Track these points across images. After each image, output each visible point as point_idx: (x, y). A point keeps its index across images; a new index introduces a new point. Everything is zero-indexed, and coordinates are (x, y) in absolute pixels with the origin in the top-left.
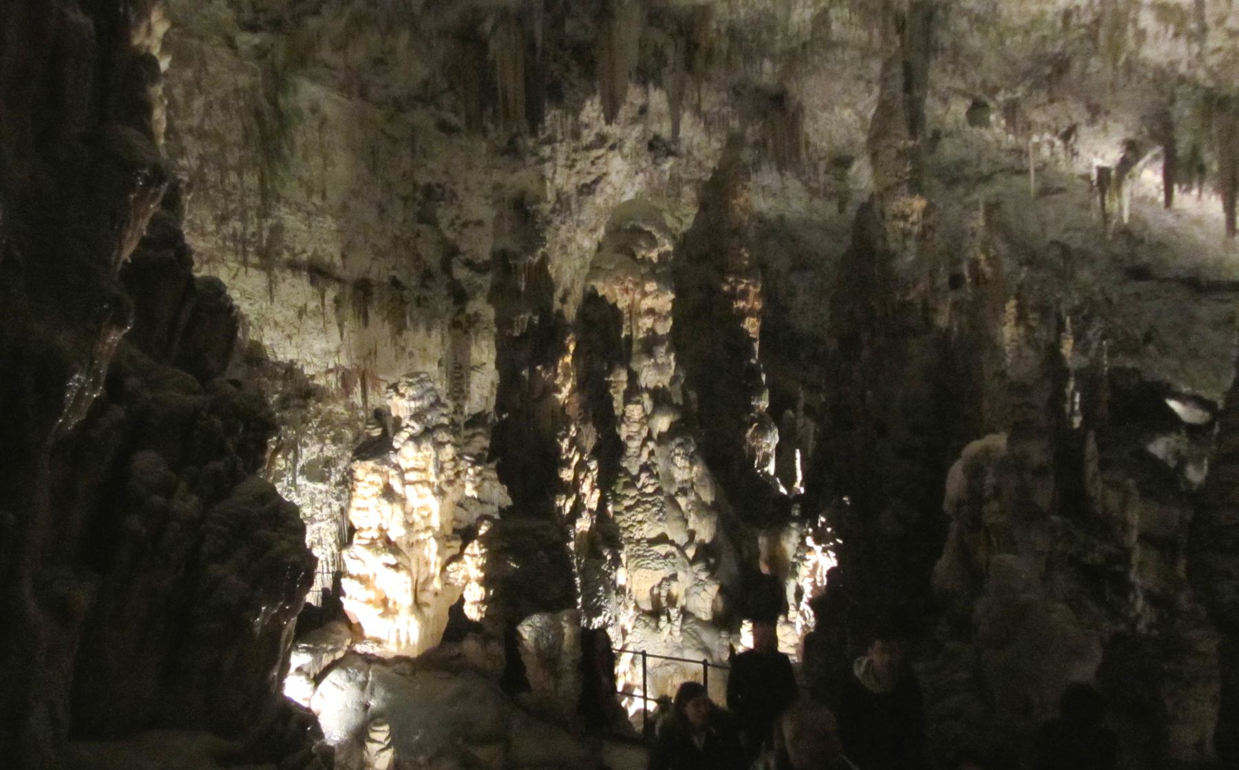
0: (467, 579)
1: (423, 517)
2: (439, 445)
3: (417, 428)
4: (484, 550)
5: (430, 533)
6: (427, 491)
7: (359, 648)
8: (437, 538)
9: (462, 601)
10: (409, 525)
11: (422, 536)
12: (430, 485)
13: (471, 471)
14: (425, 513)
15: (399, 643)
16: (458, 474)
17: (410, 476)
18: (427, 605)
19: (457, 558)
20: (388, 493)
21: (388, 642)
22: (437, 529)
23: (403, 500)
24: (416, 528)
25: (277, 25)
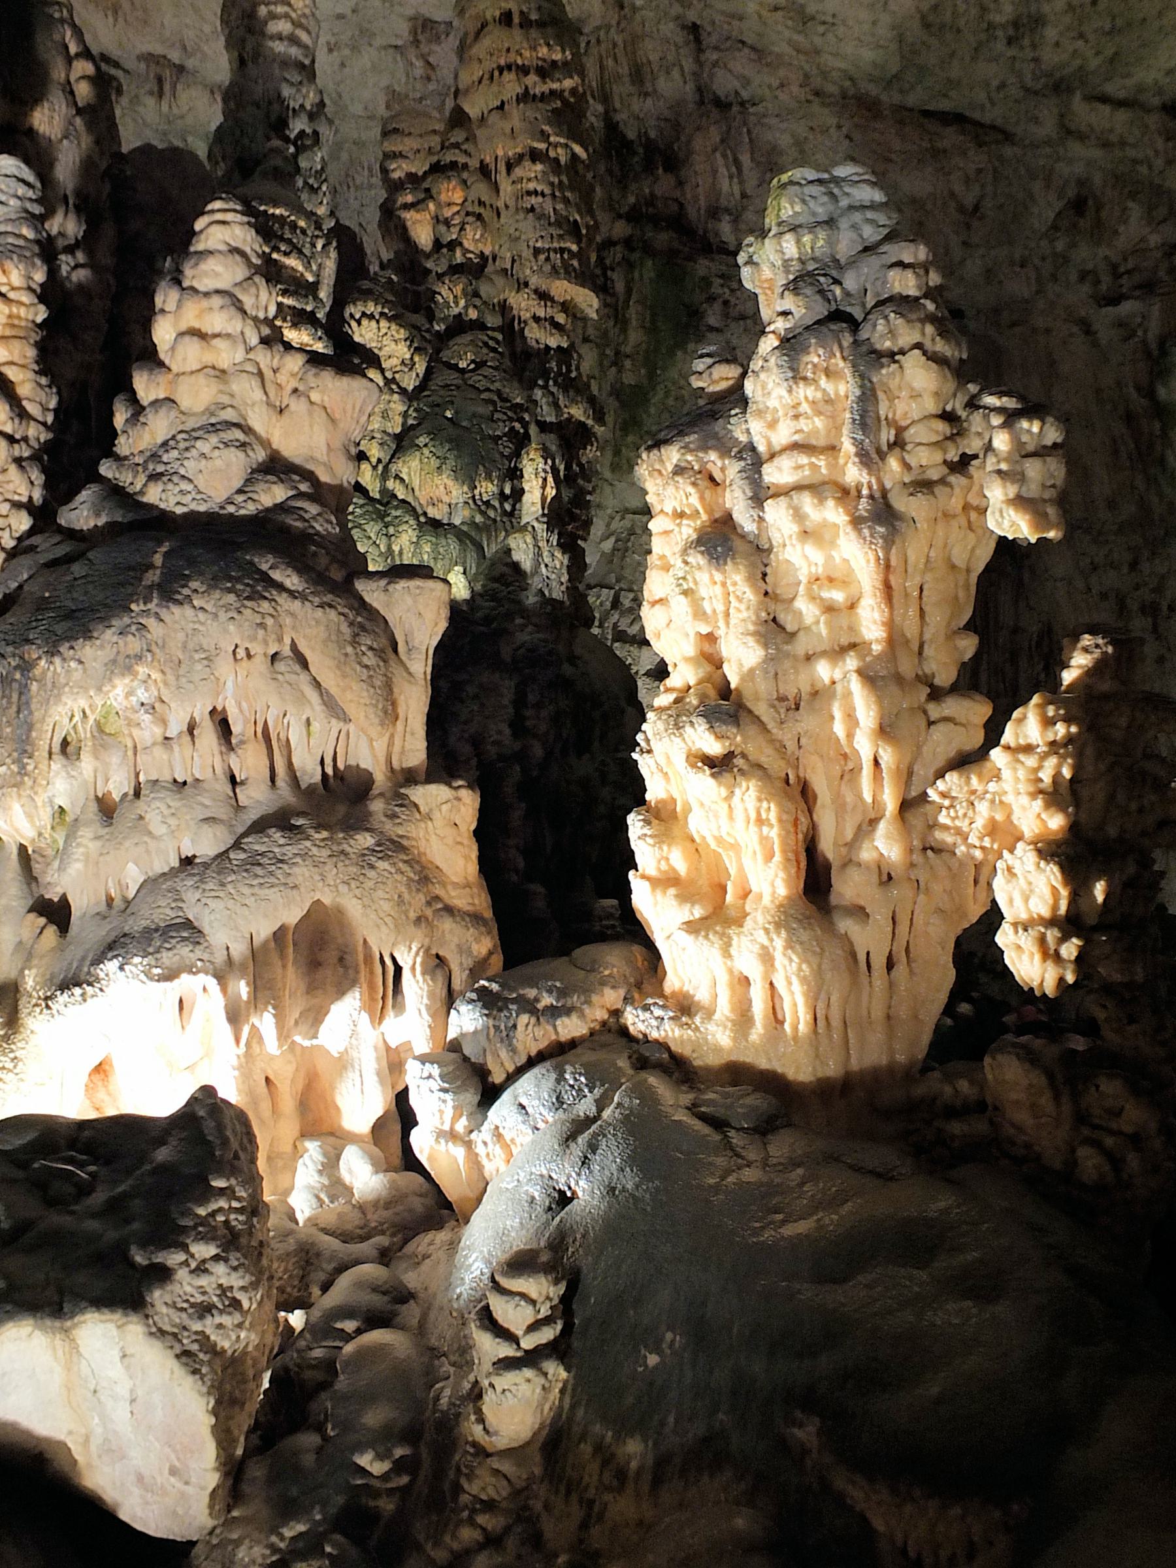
0: (1004, 833)
1: (830, 609)
2: (870, 359)
3: (800, 309)
4: (1061, 729)
5: (851, 662)
6: (833, 514)
7: (637, 1021)
8: (868, 677)
9: (993, 917)
10: (774, 629)
11: (824, 671)
12: (845, 494)
13: (1002, 442)
14: (838, 596)
15: (743, 1018)
16: (962, 464)
17: (777, 473)
18: (860, 912)
19: (968, 760)
20: (719, 539)
21: (710, 1014)
22: (877, 648)
23: (759, 555)
24: (801, 646)
25: (1148, 288)
